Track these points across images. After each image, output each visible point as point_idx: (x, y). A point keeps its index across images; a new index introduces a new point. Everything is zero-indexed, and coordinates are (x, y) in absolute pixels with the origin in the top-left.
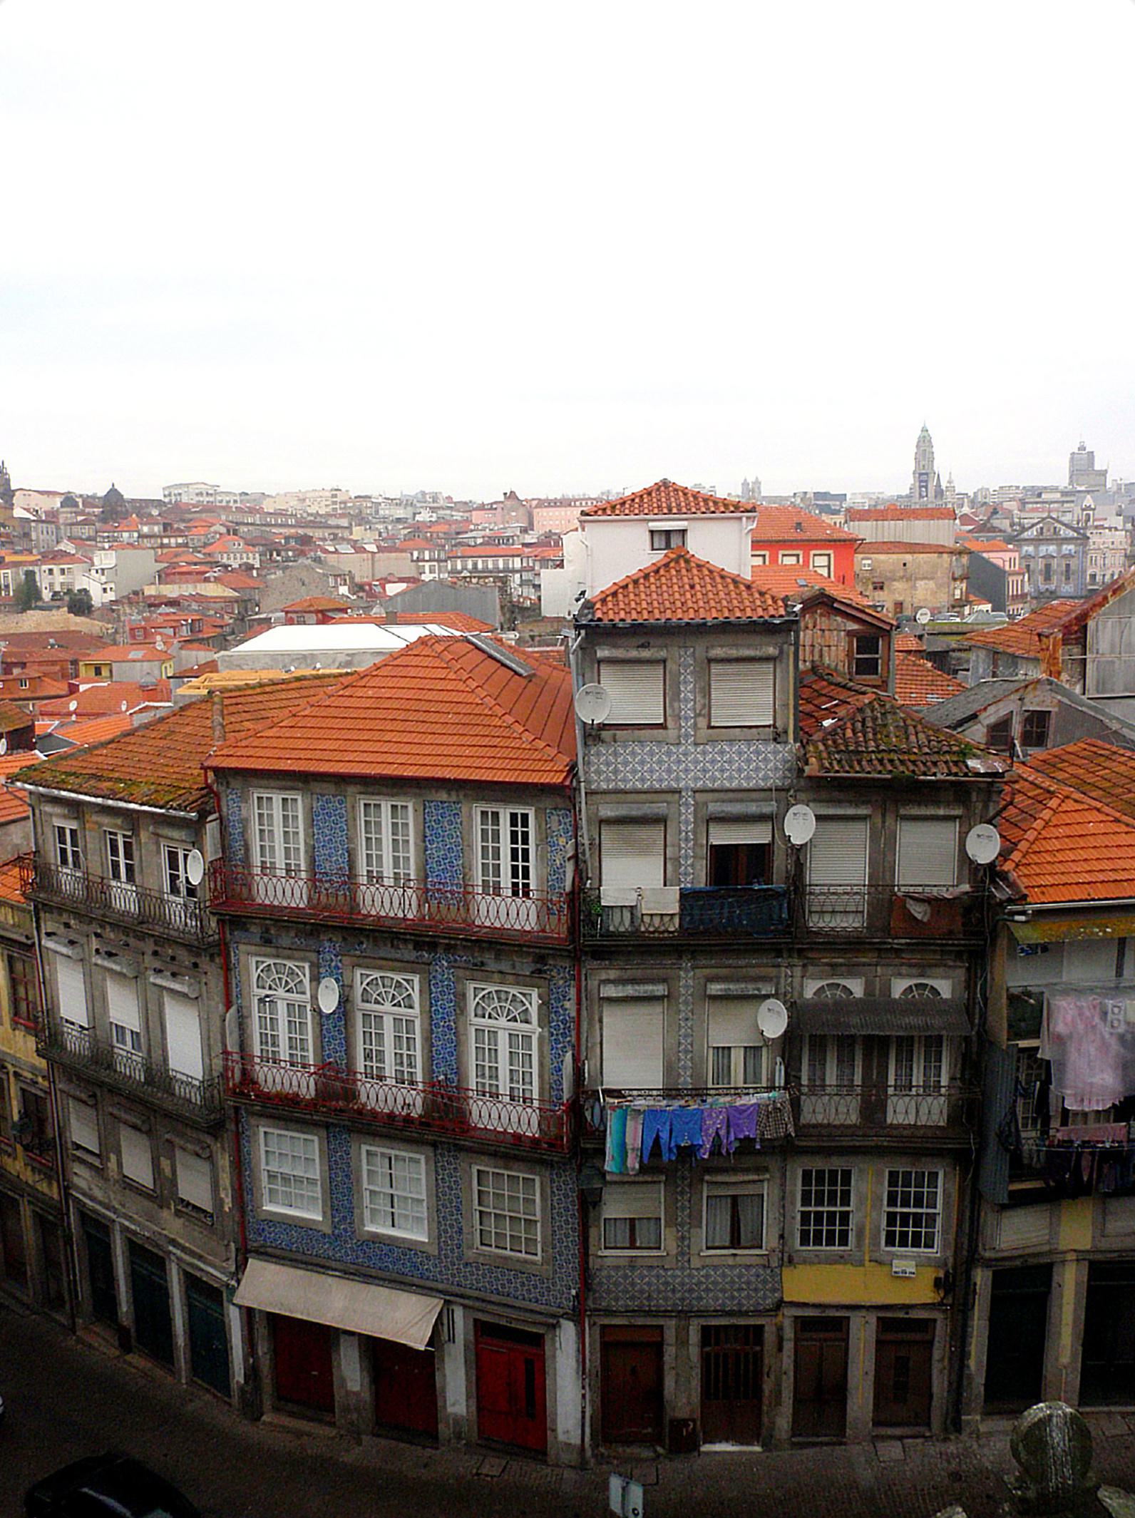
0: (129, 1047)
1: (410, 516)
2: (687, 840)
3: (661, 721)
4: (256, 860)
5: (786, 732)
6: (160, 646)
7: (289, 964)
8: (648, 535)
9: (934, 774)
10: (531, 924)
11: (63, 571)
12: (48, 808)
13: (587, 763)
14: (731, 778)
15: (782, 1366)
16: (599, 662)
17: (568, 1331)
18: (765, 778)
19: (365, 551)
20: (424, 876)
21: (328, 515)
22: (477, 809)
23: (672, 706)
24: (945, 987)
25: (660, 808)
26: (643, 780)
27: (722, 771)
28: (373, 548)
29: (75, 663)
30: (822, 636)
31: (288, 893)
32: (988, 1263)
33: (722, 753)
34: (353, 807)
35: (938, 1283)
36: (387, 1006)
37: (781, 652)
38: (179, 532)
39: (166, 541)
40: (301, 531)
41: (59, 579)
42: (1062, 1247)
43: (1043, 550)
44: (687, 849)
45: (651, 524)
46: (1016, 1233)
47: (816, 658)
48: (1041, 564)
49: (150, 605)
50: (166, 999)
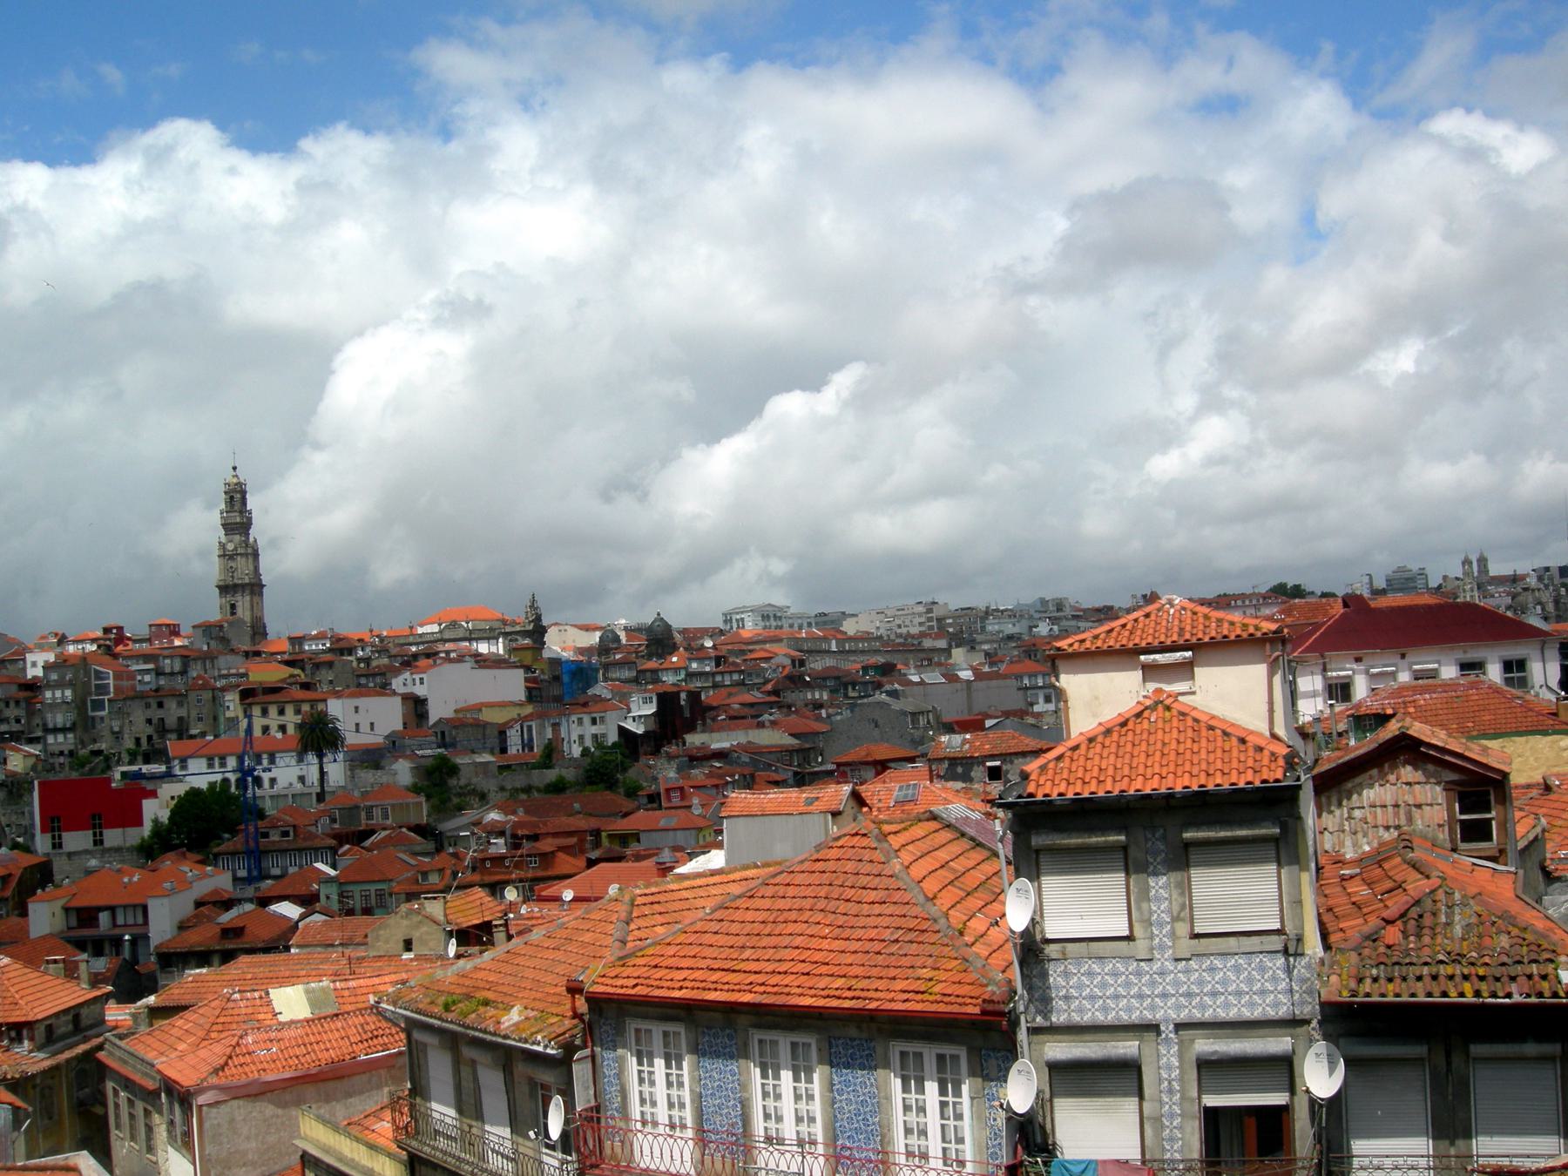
1: (1025, 630)
2: (1171, 1091)
3: (1126, 933)
4: (635, 1110)
6: (697, 811)
8: (1138, 675)
9: (1509, 995)
11: (594, 722)
12: (416, 1035)
14: (1227, 1005)
16: (1037, 852)
18: (1276, 1005)
19: (956, 679)
20: (832, 1137)
21: (922, 635)
22: (896, 1048)
23: (1139, 909)
25: (1126, 1047)
26: (1105, 1009)
27: (1214, 994)
28: (966, 675)
29: (597, 833)
30: (1413, 793)
31: (677, 1155)
34: (746, 1045)
37: (1284, 827)
39: (719, 678)
44: (1172, 1104)
45: (1142, 658)
47: (1403, 821)
49: (692, 759)
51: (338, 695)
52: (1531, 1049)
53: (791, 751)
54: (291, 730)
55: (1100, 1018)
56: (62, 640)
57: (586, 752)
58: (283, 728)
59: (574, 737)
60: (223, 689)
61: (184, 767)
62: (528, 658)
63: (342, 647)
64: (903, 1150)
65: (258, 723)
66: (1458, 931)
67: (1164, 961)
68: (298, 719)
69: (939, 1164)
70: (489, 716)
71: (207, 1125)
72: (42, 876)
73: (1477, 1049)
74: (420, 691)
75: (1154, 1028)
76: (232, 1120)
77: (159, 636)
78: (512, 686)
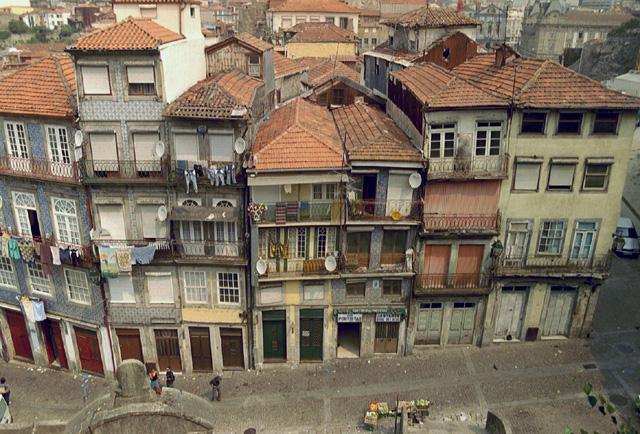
5: (161, 97)
15: (185, 345)
16: (81, 66)
17: (103, 332)
22: (47, 127)
24: (234, 203)
32: (259, 308)
33: (136, 105)
35: (240, 315)
37: (155, 62)
41: (56, 20)
42: (288, 303)
43: (489, 19)
46: (267, 298)
48: (487, 25)
52: (225, 132)
55: (103, 119)
57: (56, 28)
59: (50, 22)
66: (211, 96)
67: (121, 102)
70: (14, 11)
73: (210, 131)
75: (119, 121)
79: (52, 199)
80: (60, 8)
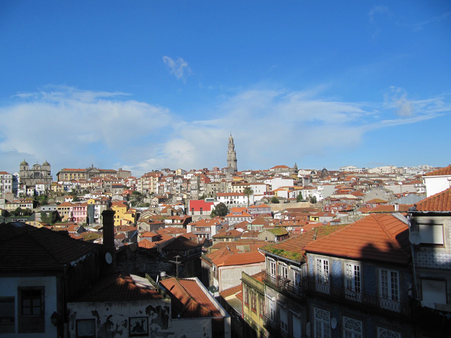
0: (284, 329)
6: (333, 212)
7: (325, 311)
10: (398, 310)
11: (309, 191)
13: (416, 258)
19: (398, 184)
21: (388, 174)
36: (353, 330)
38: (342, 180)
39: (338, 182)
40: (378, 179)
41: (308, 193)
50: (293, 316)
51: (252, 184)
53: (356, 200)
54: (242, 192)
56: (195, 171)
58: (240, 191)
60: (228, 182)
61: (219, 198)
62: (294, 177)
63: (254, 173)
64: (382, 294)
65: (235, 189)
68: (244, 189)
69: (391, 299)
71: (222, 274)
72: (189, 220)
74: (270, 184)
76: (227, 274)
77: (215, 171)
78: (290, 183)
79: (378, 328)
80: (310, 186)
